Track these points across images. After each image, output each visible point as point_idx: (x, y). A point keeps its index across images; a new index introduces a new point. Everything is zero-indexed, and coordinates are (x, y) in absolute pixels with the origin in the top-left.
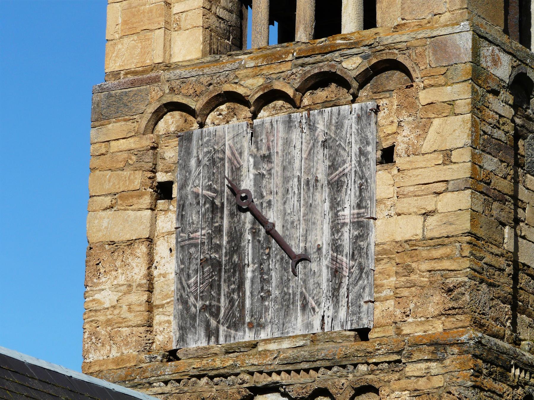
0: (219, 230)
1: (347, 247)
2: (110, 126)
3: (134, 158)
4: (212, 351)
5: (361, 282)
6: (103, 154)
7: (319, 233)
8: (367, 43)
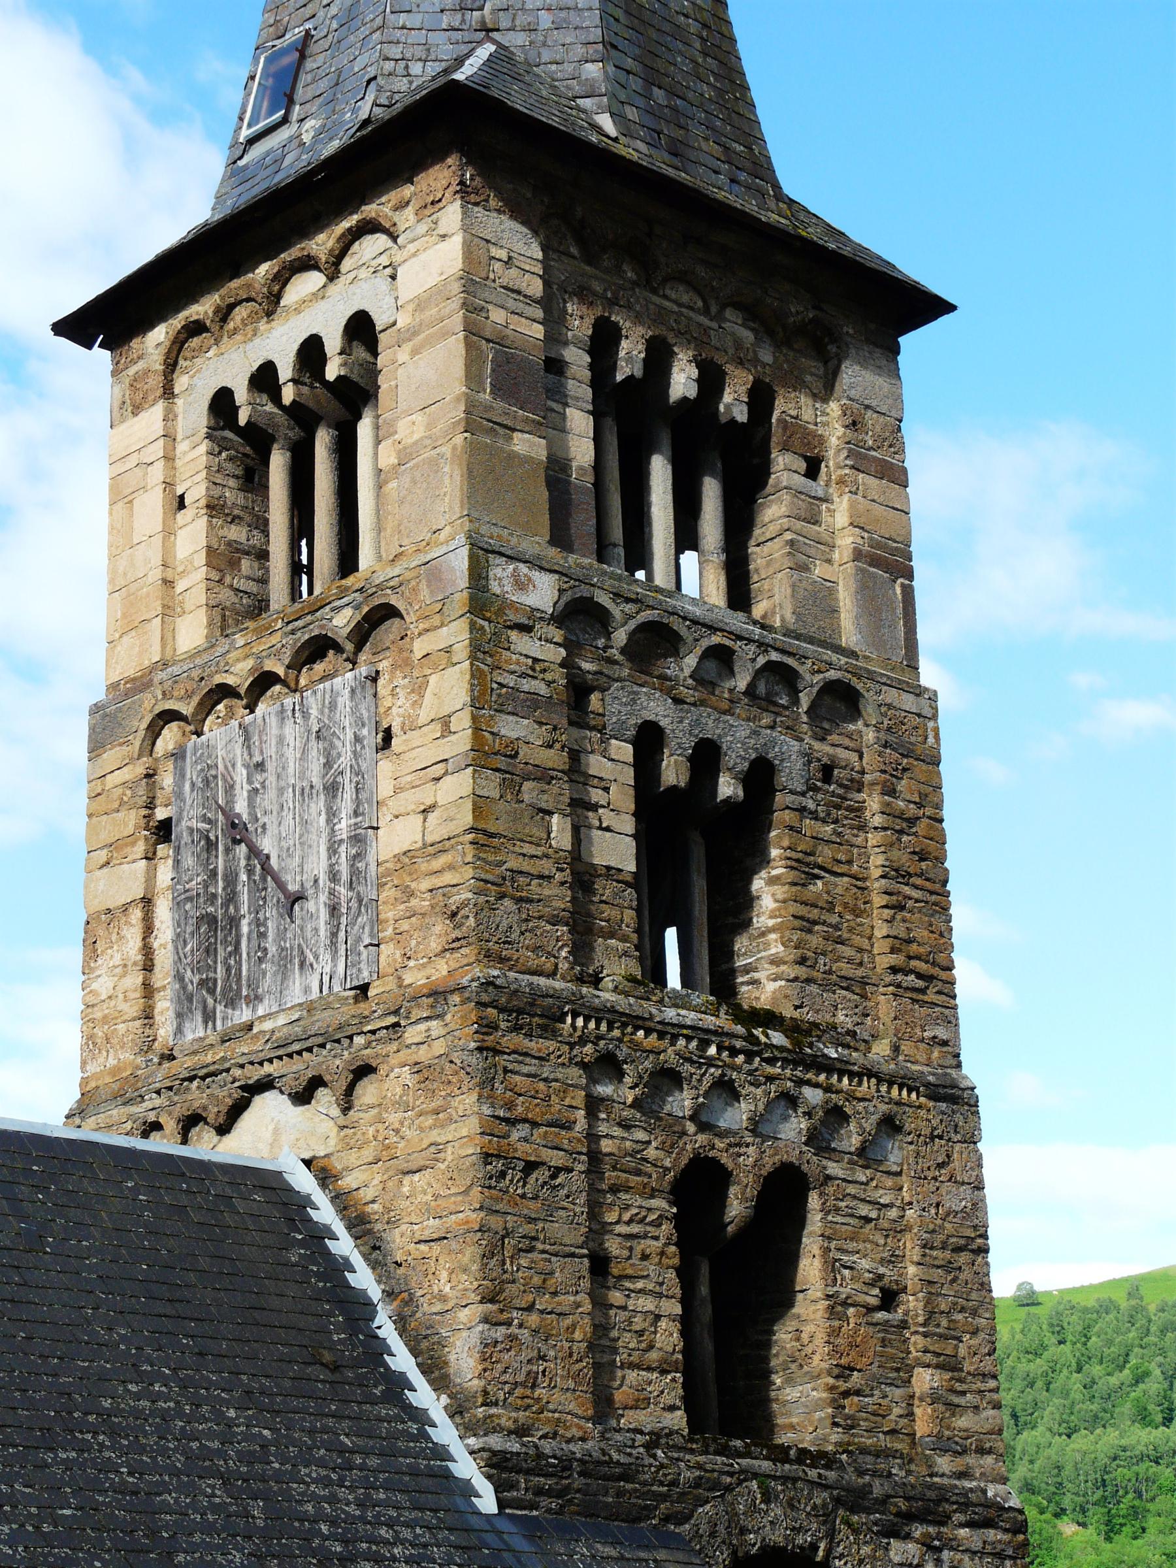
0: (213, 874)
1: (345, 876)
2: (105, 756)
3: (129, 792)
4: (208, 1042)
5: (360, 919)
6: (99, 794)
7: (315, 859)
8: (355, 588)
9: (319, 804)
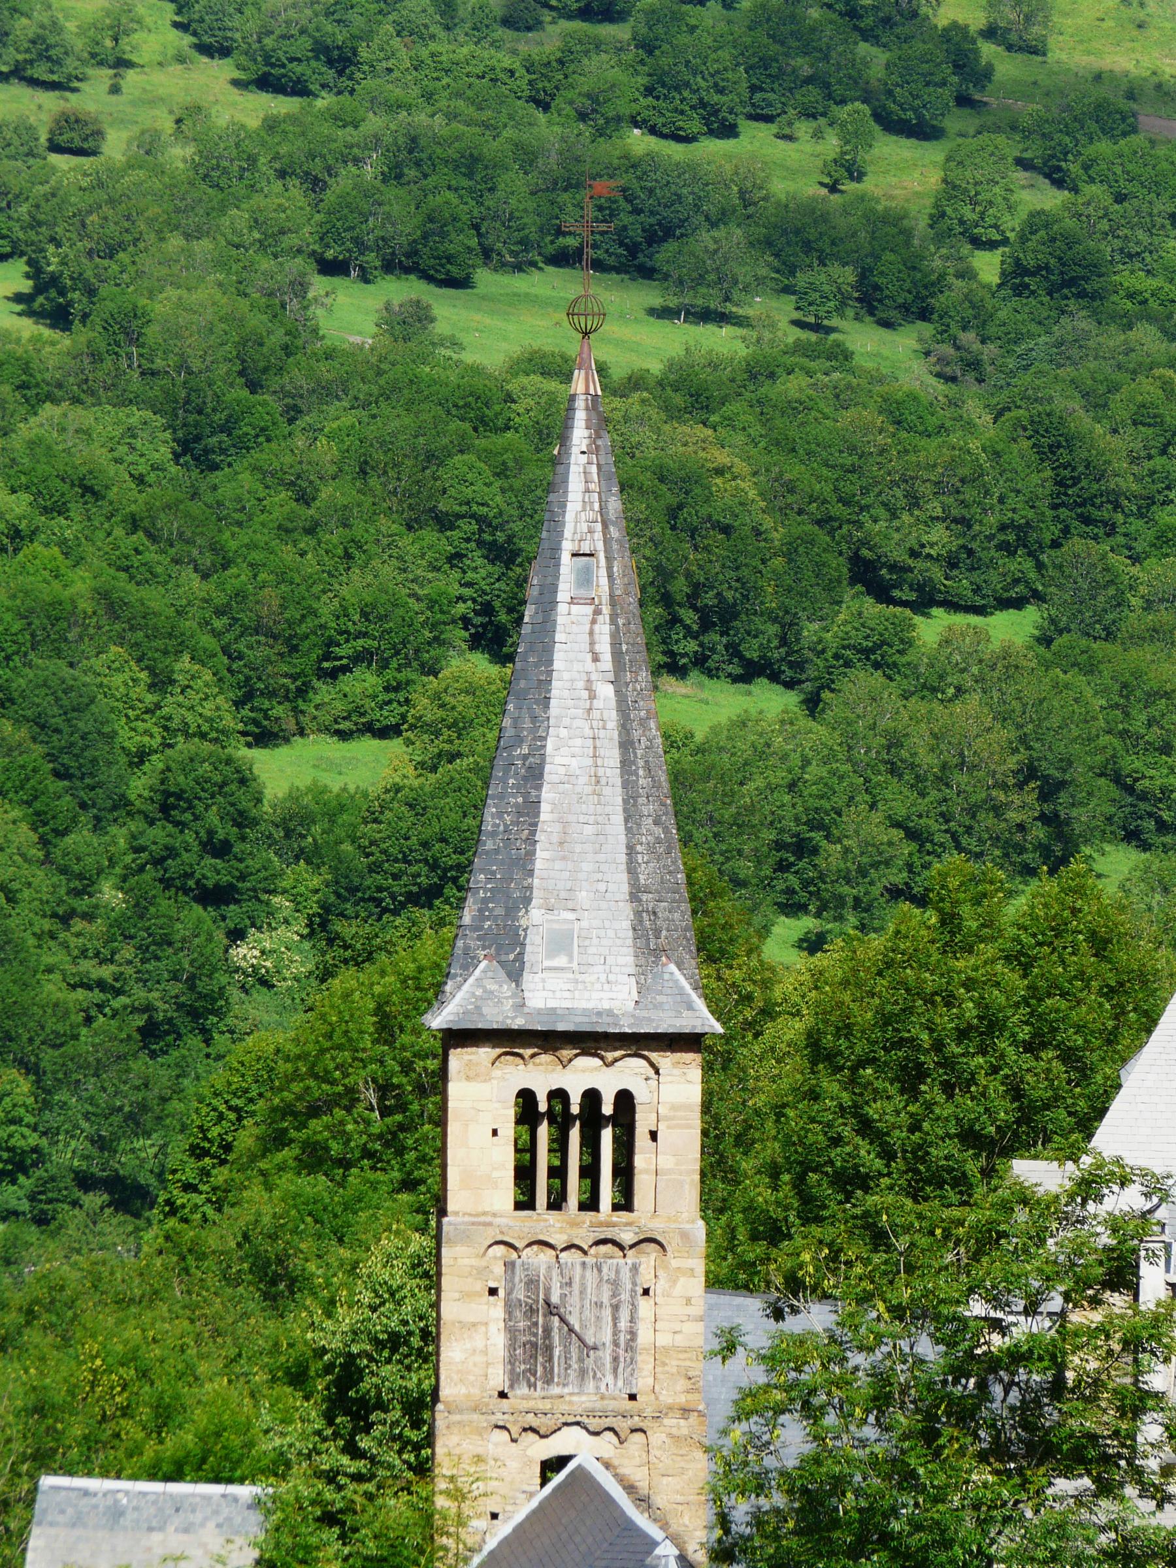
9: (607, 1313)
